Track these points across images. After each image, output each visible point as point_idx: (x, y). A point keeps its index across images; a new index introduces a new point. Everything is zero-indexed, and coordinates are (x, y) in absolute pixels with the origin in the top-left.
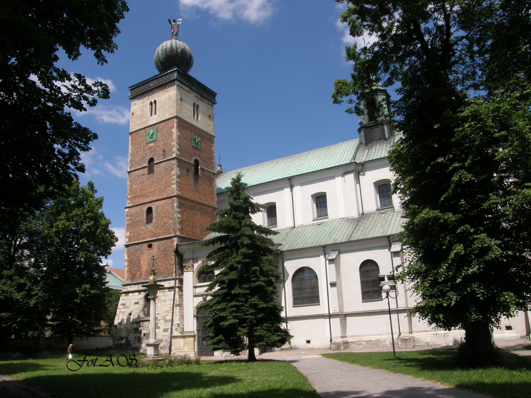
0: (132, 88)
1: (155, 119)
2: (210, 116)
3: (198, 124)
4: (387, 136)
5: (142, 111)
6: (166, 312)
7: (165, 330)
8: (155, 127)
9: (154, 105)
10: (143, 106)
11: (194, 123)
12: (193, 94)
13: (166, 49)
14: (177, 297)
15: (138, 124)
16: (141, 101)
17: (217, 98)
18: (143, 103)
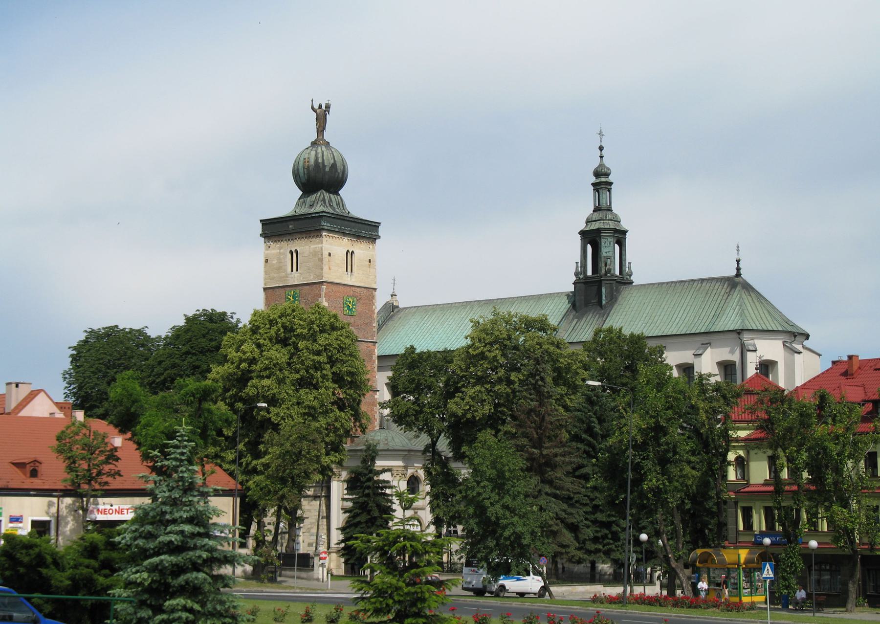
0: (265, 223)
1: (296, 278)
2: (370, 261)
3: (353, 280)
4: (604, 302)
5: (279, 259)
6: (311, 523)
7: (310, 545)
8: (298, 290)
9: (295, 255)
10: (280, 254)
11: (348, 280)
12: (346, 240)
13: (308, 167)
14: (324, 508)
15: (273, 278)
16: (278, 245)
17: (381, 231)
18: (280, 248)
